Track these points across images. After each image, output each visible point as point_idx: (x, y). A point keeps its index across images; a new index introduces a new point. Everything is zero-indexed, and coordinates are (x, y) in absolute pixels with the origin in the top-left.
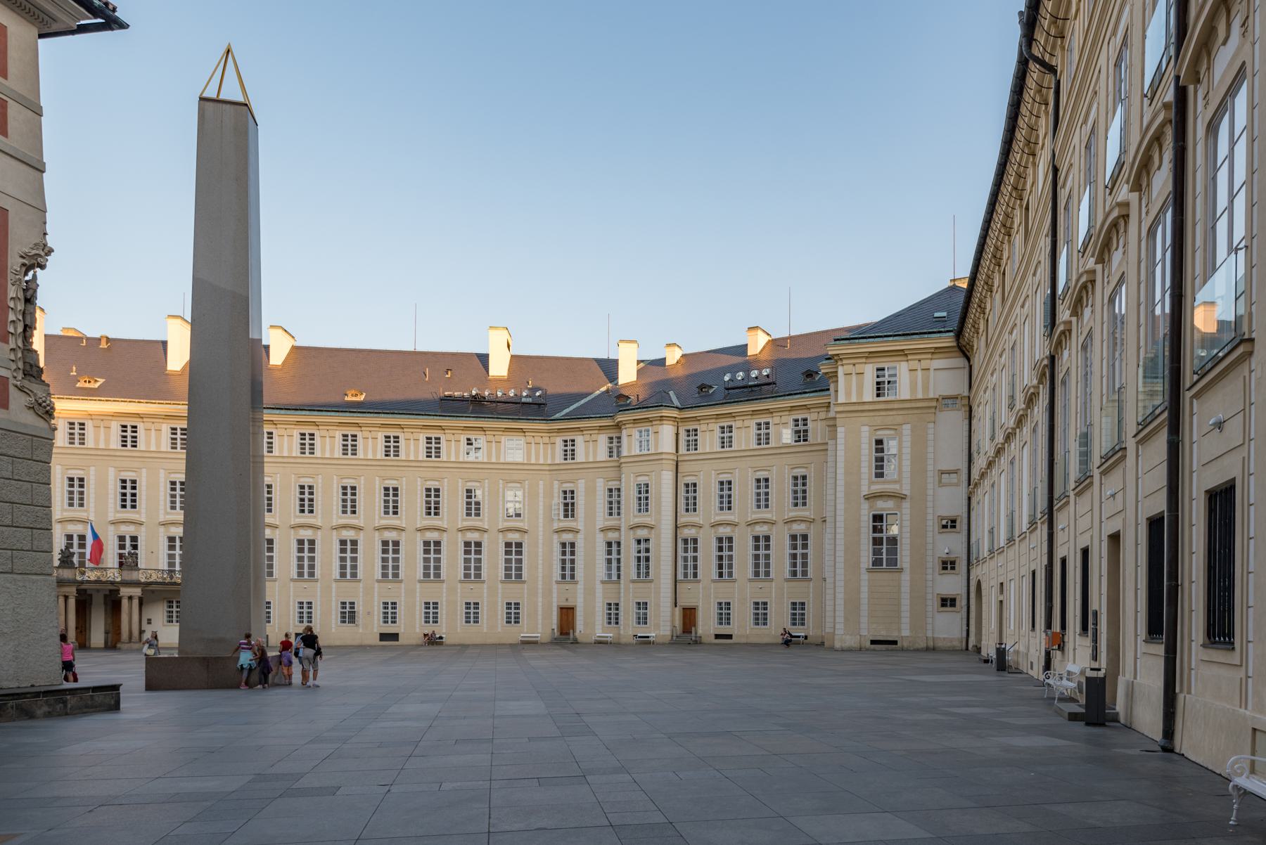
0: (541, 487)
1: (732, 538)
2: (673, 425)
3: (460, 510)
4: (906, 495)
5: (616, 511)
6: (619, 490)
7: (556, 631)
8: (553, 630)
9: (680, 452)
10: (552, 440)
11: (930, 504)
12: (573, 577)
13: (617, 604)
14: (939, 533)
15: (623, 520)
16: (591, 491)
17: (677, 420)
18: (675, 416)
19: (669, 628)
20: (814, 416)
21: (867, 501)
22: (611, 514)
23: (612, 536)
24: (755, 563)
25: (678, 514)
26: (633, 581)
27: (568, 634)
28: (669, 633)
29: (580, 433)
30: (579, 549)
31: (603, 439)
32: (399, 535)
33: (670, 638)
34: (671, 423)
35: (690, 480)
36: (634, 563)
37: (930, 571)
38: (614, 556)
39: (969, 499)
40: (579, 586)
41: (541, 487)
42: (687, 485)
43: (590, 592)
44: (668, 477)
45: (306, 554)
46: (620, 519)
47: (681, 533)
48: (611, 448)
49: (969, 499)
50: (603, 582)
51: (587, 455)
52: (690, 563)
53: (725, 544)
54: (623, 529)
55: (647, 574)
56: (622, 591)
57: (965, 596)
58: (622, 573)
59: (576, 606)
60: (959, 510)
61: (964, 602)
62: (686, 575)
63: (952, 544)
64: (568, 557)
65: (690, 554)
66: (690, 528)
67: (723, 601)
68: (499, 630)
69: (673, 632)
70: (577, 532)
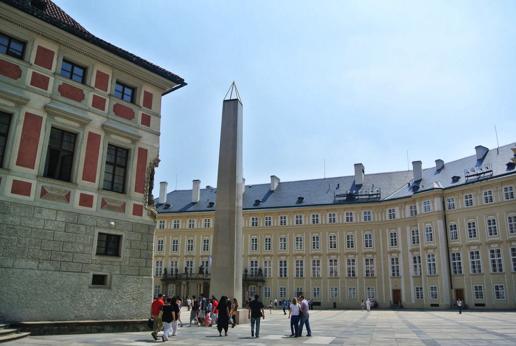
0: (381, 232)
3: (345, 245)
5: (417, 241)
7: (392, 302)
8: (391, 301)
12: (398, 275)
15: (420, 246)
16: (404, 232)
19: (449, 300)
22: (414, 243)
24: (493, 264)
26: (428, 276)
27: (398, 303)
28: (449, 303)
31: (408, 208)
32: (320, 258)
33: (450, 306)
35: (452, 223)
36: (427, 267)
41: (381, 232)
43: (407, 282)
44: (440, 223)
45: (283, 267)
46: (419, 245)
54: (420, 250)
56: (423, 281)
58: (422, 272)
59: (401, 289)
62: (456, 272)
67: (478, 286)
68: (329, 301)
69: (451, 302)
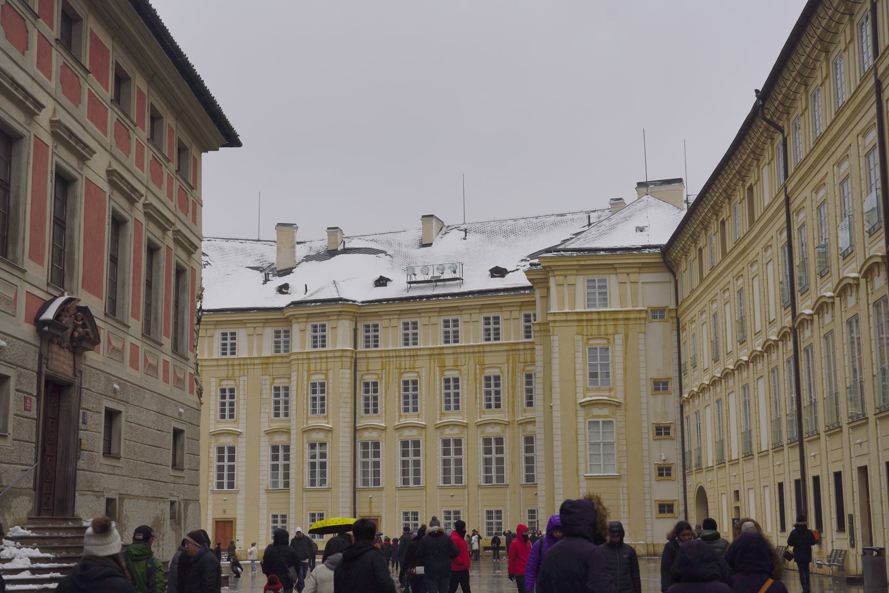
1: (378, 443)
2: (351, 320)
4: (621, 403)
6: (287, 389)
9: (359, 349)
10: (210, 333)
11: (644, 412)
13: (284, 516)
14: (654, 440)
15: (294, 422)
17: (356, 315)
18: (355, 310)
20: (507, 315)
21: (583, 409)
22: (277, 415)
23: (280, 440)
25: (357, 416)
29: (243, 326)
30: (240, 455)
31: (269, 334)
34: (350, 317)
35: (370, 379)
37: (647, 478)
38: (281, 462)
39: (682, 407)
40: (238, 496)
42: (367, 385)
47: (360, 437)
48: (276, 342)
49: (682, 407)
50: (267, 491)
51: (251, 350)
52: (371, 469)
53: (412, 448)
54: (293, 432)
55: (323, 482)
56: (292, 501)
57: (682, 502)
59: (235, 519)
60: (671, 417)
61: (682, 508)
62: (365, 482)
63: (667, 451)
64: (226, 463)
65: (371, 459)
66: (370, 430)
70: (238, 435)
